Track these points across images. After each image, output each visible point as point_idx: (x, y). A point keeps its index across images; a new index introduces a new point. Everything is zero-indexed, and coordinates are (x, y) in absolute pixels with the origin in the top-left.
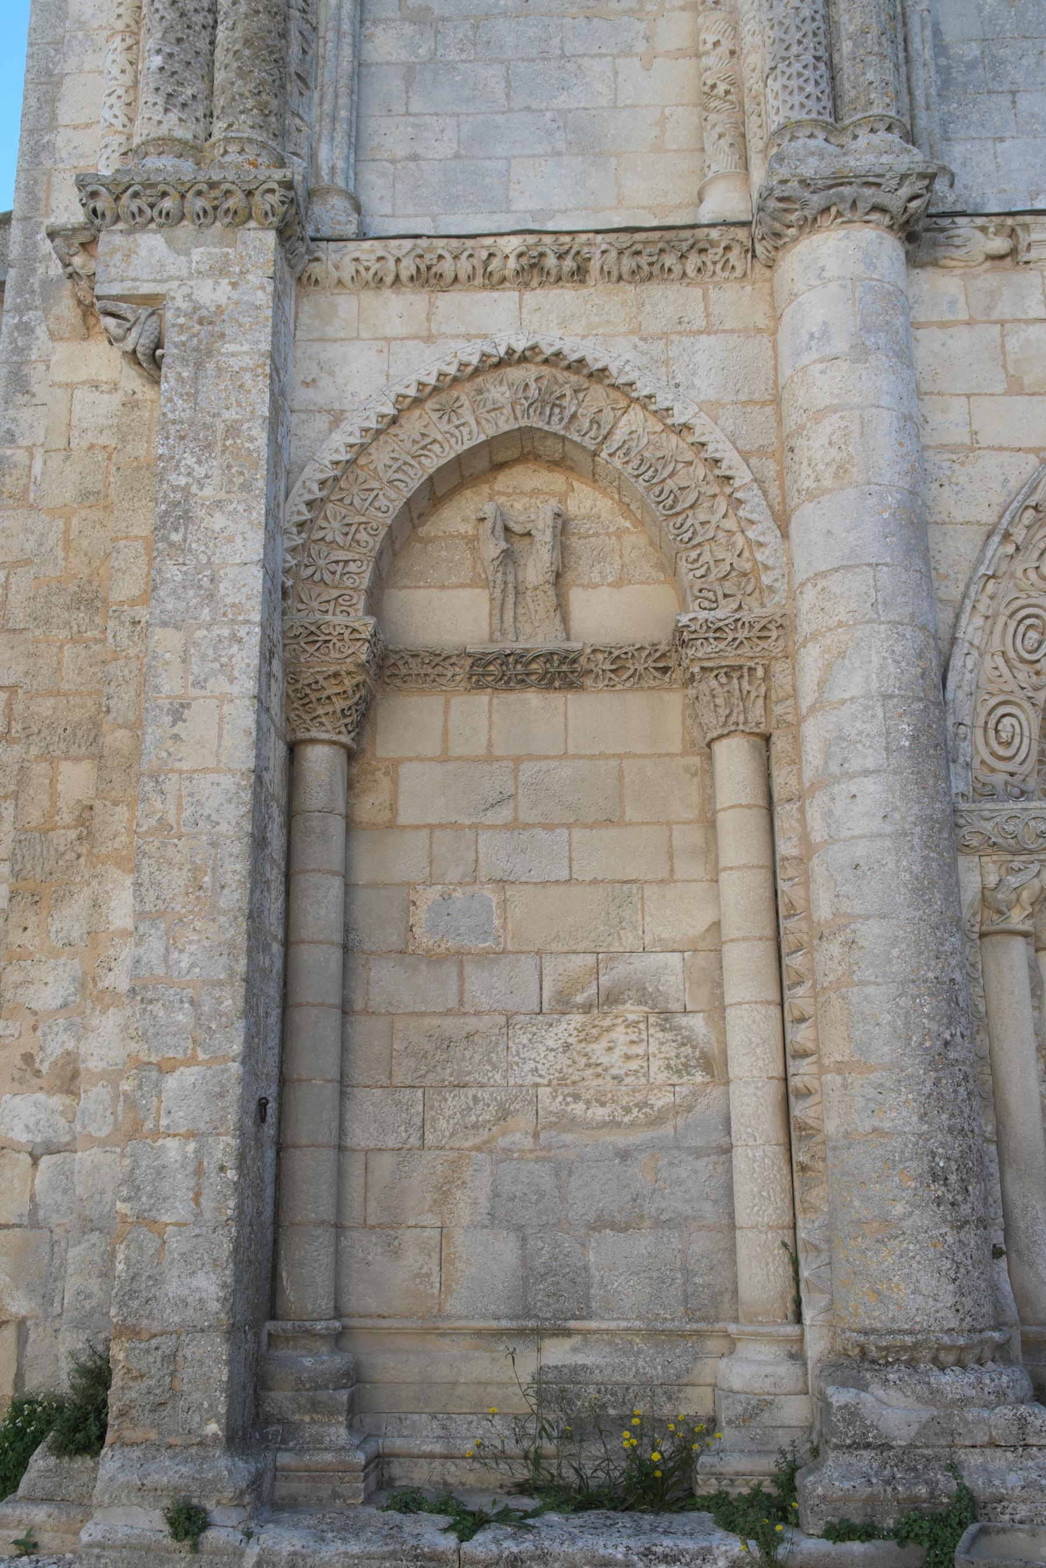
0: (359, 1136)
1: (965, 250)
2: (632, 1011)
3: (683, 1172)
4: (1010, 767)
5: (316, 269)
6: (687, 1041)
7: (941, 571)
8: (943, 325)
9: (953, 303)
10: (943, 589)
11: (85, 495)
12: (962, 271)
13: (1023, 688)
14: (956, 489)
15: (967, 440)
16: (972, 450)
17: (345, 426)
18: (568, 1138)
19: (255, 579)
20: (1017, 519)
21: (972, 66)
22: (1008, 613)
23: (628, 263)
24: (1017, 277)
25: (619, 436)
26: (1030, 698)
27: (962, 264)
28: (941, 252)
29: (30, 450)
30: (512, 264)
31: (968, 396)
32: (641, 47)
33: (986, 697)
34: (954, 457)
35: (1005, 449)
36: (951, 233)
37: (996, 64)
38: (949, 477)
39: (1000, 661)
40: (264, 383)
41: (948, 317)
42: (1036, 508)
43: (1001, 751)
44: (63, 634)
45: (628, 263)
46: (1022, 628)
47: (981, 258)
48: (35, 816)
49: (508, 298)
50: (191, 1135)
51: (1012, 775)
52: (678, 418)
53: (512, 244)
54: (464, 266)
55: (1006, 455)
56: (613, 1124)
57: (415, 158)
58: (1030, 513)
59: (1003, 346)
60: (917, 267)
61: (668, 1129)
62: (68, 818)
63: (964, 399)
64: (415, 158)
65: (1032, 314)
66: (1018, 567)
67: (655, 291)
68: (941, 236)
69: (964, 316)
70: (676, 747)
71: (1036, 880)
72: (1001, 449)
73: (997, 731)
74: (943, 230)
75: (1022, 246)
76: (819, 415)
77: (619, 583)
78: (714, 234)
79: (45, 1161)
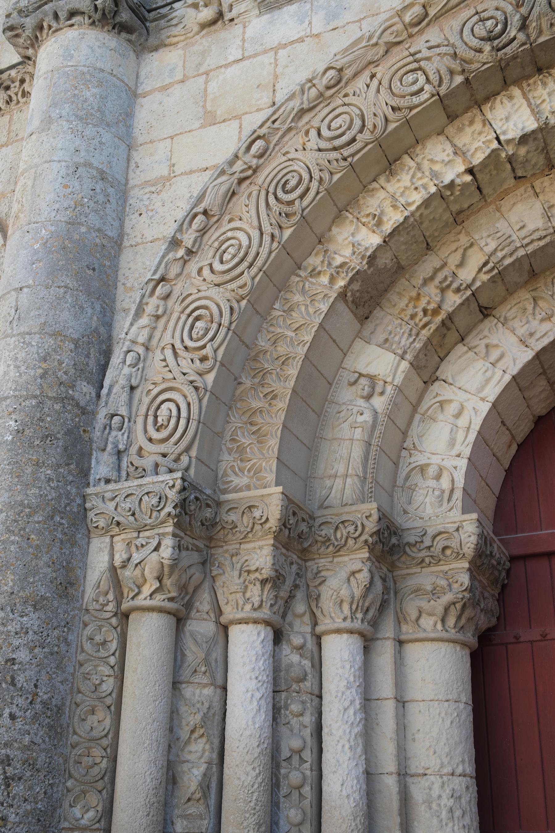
1: (181, 26)
4: (162, 448)
7: (128, 285)
8: (165, 88)
9: (173, 70)
10: (127, 300)
12: (185, 43)
13: (184, 374)
14: (150, 214)
15: (165, 173)
16: (168, 179)
20: (185, 226)
22: (180, 309)
24: (223, 34)
26: (191, 382)
27: (182, 38)
28: (165, 33)
31: (172, 138)
33: (152, 387)
34: (153, 189)
35: (194, 172)
36: (169, 17)
38: (147, 206)
39: (169, 352)
41: (168, 81)
42: (205, 213)
43: (156, 435)
46: (191, 320)
47: (196, 28)
51: (164, 455)
55: (195, 176)
58: (200, 218)
59: (206, 90)
60: (152, 51)
63: (170, 140)
65: (231, 58)
66: (192, 267)
68: (163, 22)
69: (179, 77)
71: (155, 553)
72: (191, 172)
73: (156, 417)
74: (164, 16)
75: (225, 8)
78: (13, 73)
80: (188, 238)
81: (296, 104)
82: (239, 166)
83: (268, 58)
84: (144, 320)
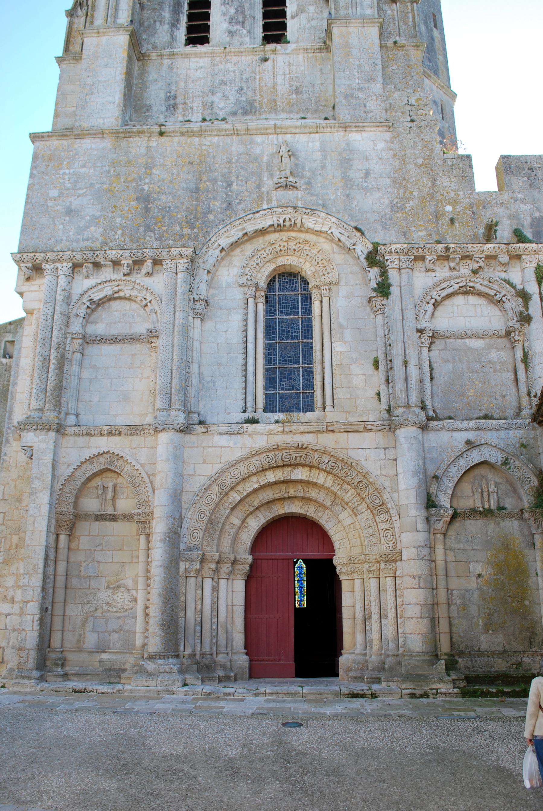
0: (68, 613)
2: (122, 589)
3: (129, 621)
5: (66, 432)
6: (132, 596)
8: (192, 447)
11: (19, 476)
17: (70, 468)
18: (108, 614)
19: (47, 507)
21: (209, 382)
23: (129, 432)
25: (125, 470)
29: (10, 457)
30: (106, 432)
32: (140, 376)
37: (214, 382)
40: (51, 465)
44: (14, 507)
45: (129, 432)
48: (8, 547)
49: (105, 439)
50: (32, 615)
52: (136, 468)
53: (106, 428)
54: (96, 432)
56: (117, 612)
57: (90, 401)
61: (127, 613)
62: (14, 547)
64: (90, 401)
66: (201, 500)
67: (134, 438)
70: (135, 534)
76: (160, 472)
77: (126, 498)
78: (147, 427)
79: (8, 617)
80: (201, 495)
81: (227, 467)
82: (213, 479)
83: (219, 449)
84: (190, 513)
